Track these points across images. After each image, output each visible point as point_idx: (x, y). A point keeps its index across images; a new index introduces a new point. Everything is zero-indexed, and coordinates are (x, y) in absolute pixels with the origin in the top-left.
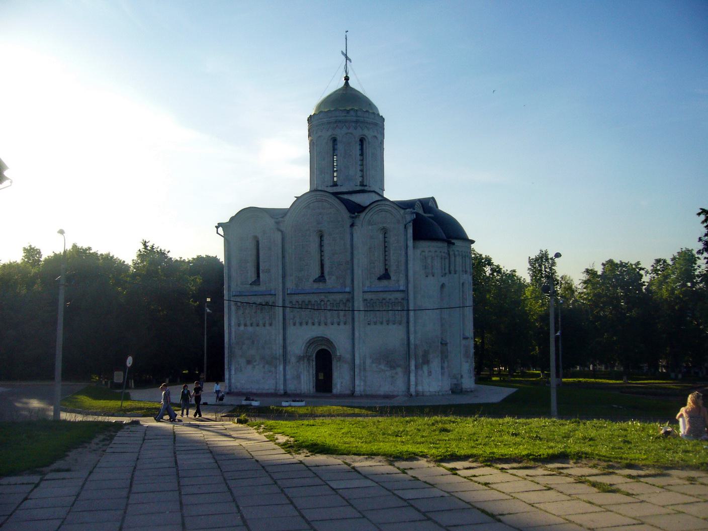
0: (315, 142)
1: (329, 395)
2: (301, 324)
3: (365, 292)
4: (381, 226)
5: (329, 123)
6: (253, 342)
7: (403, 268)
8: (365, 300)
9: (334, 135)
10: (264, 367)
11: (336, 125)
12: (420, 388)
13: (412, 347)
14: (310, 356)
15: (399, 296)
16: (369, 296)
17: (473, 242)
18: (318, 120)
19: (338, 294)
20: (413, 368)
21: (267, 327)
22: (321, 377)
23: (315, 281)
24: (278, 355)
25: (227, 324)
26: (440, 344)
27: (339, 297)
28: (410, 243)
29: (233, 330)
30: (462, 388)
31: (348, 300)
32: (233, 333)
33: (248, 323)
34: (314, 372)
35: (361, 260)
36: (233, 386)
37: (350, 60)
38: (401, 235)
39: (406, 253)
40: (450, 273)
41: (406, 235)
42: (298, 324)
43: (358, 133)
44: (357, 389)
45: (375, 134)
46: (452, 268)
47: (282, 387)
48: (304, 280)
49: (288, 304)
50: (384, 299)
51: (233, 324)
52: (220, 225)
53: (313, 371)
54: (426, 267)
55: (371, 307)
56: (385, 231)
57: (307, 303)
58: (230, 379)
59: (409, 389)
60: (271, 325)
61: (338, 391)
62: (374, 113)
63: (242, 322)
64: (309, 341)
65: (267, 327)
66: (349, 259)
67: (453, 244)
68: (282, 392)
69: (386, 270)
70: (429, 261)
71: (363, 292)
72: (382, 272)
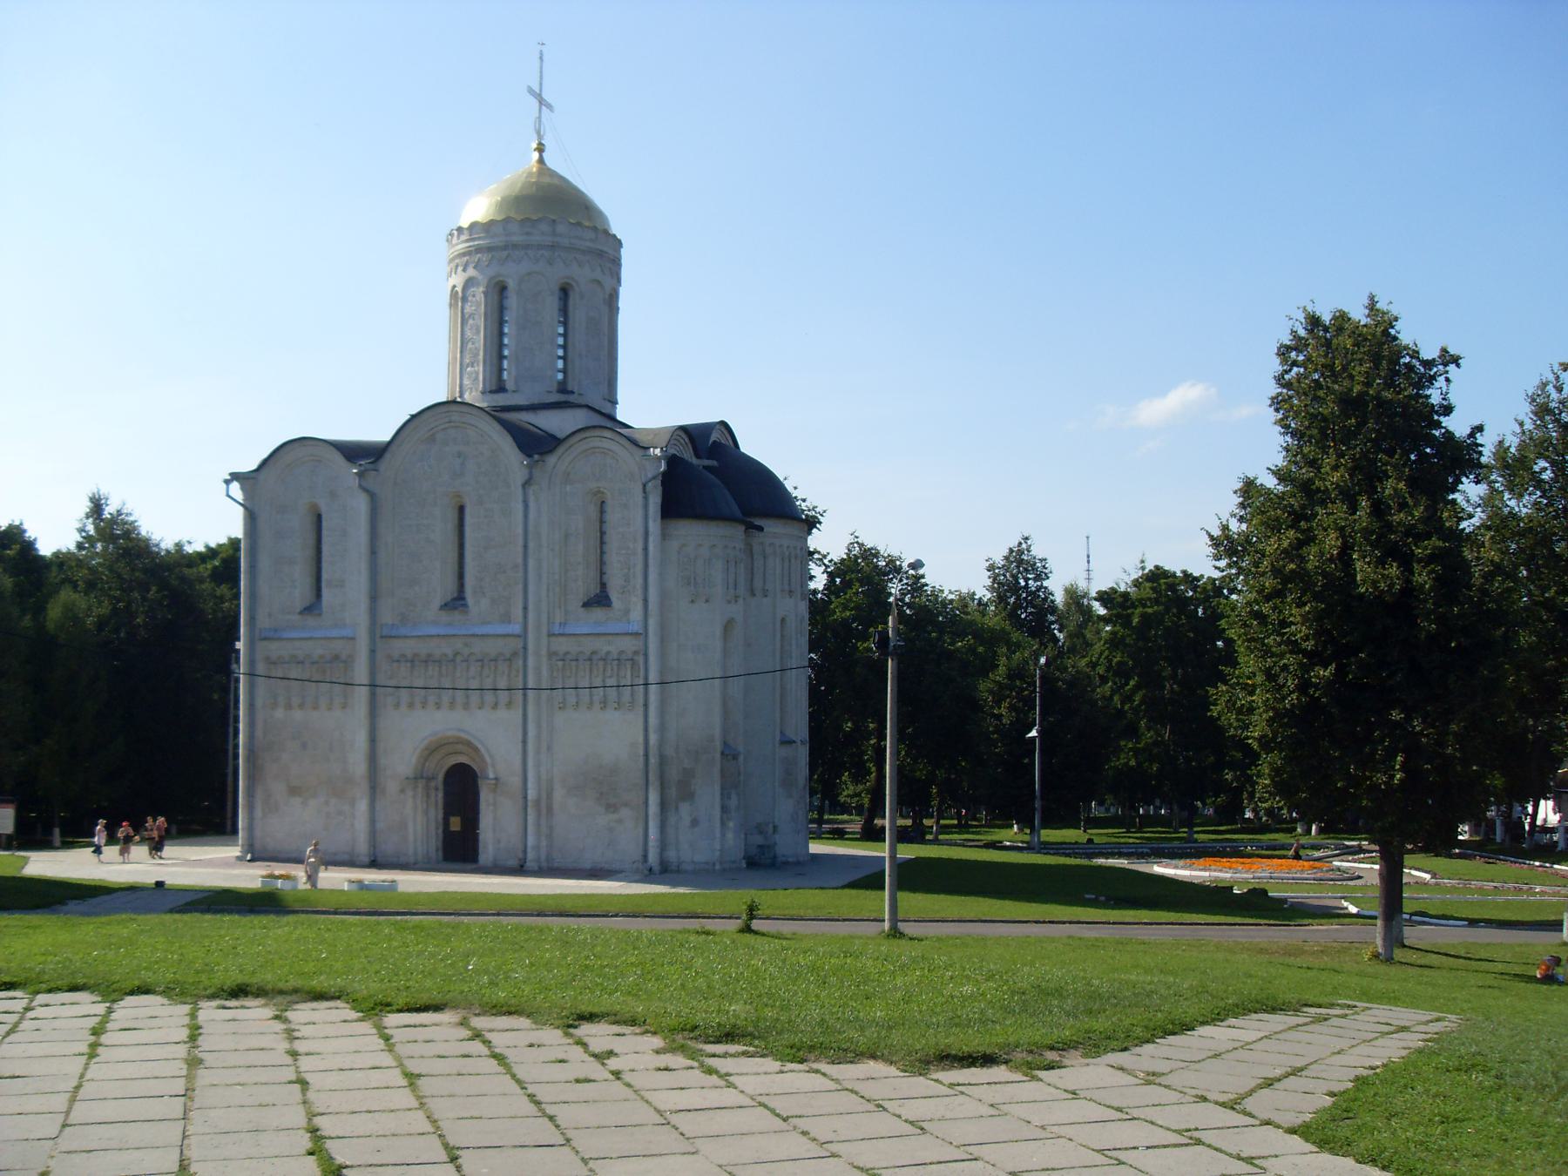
1: (469, 866)
5: (490, 249)
6: (304, 746)
7: (640, 581)
8: (552, 655)
10: (327, 803)
12: (671, 855)
13: (653, 761)
14: (429, 779)
15: (629, 645)
16: (562, 645)
17: (811, 523)
22: (456, 824)
23: (445, 606)
26: (718, 756)
28: (655, 526)
29: (260, 717)
30: (775, 857)
31: (515, 654)
34: (441, 816)
36: (258, 845)
37: (549, 107)
38: (635, 511)
39: (646, 549)
40: (753, 595)
41: (646, 507)
46: (758, 584)
49: (261, 668)
51: (259, 702)
52: (235, 476)
53: (437, 813)
59: (645, 857)
62: (595, 229)
66: (520, 560)
67: (761, 529)
72: (594, 589)
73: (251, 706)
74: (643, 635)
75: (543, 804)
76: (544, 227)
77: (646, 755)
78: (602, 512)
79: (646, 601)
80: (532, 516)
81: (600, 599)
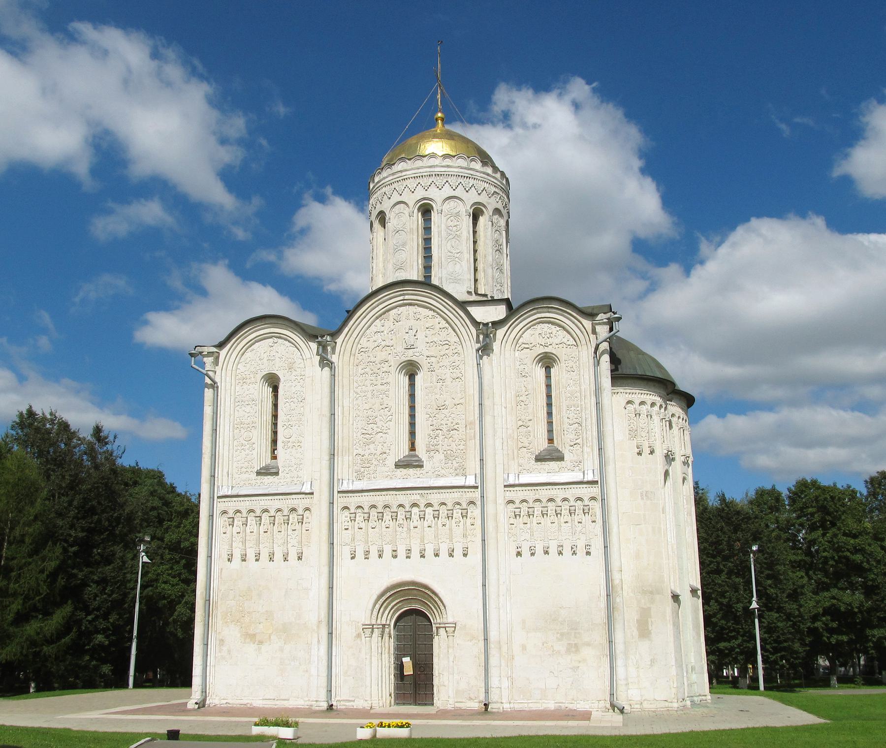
2: (367, 553)
4: (542, 350)
9: (424, 199)
11: (431, 180)
14: (384, 625)
18: (393, 174)
27: (450, 497)
33: (251, 555)
35: (501, 419)
43: (472, 197)
44: (494, 697)
45: (500, 206)
48: (376, 463)
50: (551, 500)
54: (633, 433)
56: (547, 361)
57: (380, 510)
61: (451, 701)
68: (325, 705)
69: (551, 440)
71: (505, 486)
73: (210, 557)
78: (548, 377)
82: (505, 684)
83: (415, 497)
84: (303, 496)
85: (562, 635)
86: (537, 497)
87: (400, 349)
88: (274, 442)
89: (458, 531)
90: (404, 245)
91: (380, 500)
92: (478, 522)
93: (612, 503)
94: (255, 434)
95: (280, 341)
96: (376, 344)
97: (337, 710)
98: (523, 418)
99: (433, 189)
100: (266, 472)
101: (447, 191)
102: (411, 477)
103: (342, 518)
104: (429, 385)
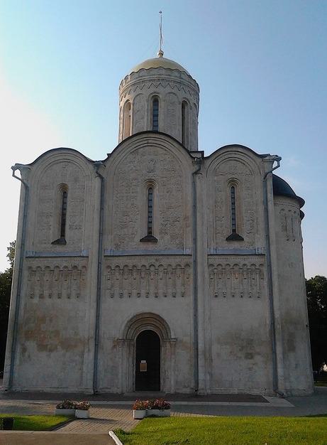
0: (131, 101)
2: (121, 296)
3: (211, 255)
7: (262, 226)
13: (278, 327)
19: (173, 257)
20: (279, 356)
21: (73, 300)
22: (144, 369)
24: (86, 337)
25: (15, 294)
28: (270, 196)
31: (187, 265)
32: (22, 307)
39: (266, 210)
41: (265, 186)
42: (117, 296)
43: (182, 95)
44: (201, 386)
47: (90, 384)
51: (23, 294)
52: (17, 167)
55: (217, 271)
56: (233, 184)
58: (12, 371)
60: (78, 296)
63: (37, 292)
64: (132, 319)
65: (73, 300)
66: (190, 213)
70: (289, 221)
72: (230, 233)
73: (18, 295)
74: (266, 255)
75: (208, 355)
76: (176, 74)
77: (273, 324)
79: (268, 237)
80: (198, 190)
81: (235, 237)
82: (208, 377)
83: (152, 260)
84: (82, 258)
85: (243, 347)
86: (228, 263)
87: (144, 172)
88: (63, 224)
89: (179, 282)
90: (143, 118)
91: (130, 262)
92: (192, 277)
93: (274, 268)
94: (52, 219)
95: (70, 164)
96: (130, 168)
97: (100, 395)
98: (219, 216)
99: (160, 87)
100: (57, 242)
101: (168, 89)
102: (150, 247)
103: (105, 272)
104: (162, 194)
